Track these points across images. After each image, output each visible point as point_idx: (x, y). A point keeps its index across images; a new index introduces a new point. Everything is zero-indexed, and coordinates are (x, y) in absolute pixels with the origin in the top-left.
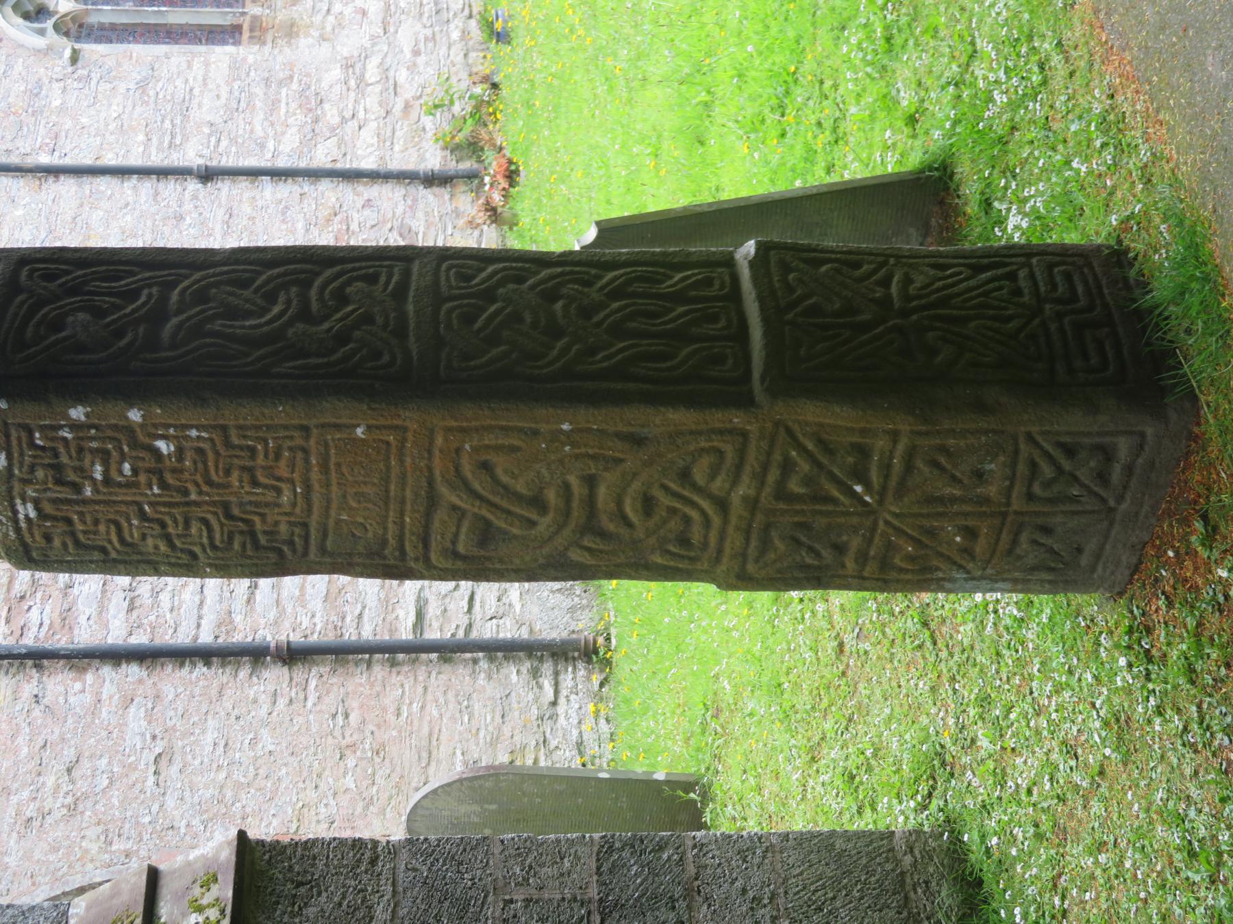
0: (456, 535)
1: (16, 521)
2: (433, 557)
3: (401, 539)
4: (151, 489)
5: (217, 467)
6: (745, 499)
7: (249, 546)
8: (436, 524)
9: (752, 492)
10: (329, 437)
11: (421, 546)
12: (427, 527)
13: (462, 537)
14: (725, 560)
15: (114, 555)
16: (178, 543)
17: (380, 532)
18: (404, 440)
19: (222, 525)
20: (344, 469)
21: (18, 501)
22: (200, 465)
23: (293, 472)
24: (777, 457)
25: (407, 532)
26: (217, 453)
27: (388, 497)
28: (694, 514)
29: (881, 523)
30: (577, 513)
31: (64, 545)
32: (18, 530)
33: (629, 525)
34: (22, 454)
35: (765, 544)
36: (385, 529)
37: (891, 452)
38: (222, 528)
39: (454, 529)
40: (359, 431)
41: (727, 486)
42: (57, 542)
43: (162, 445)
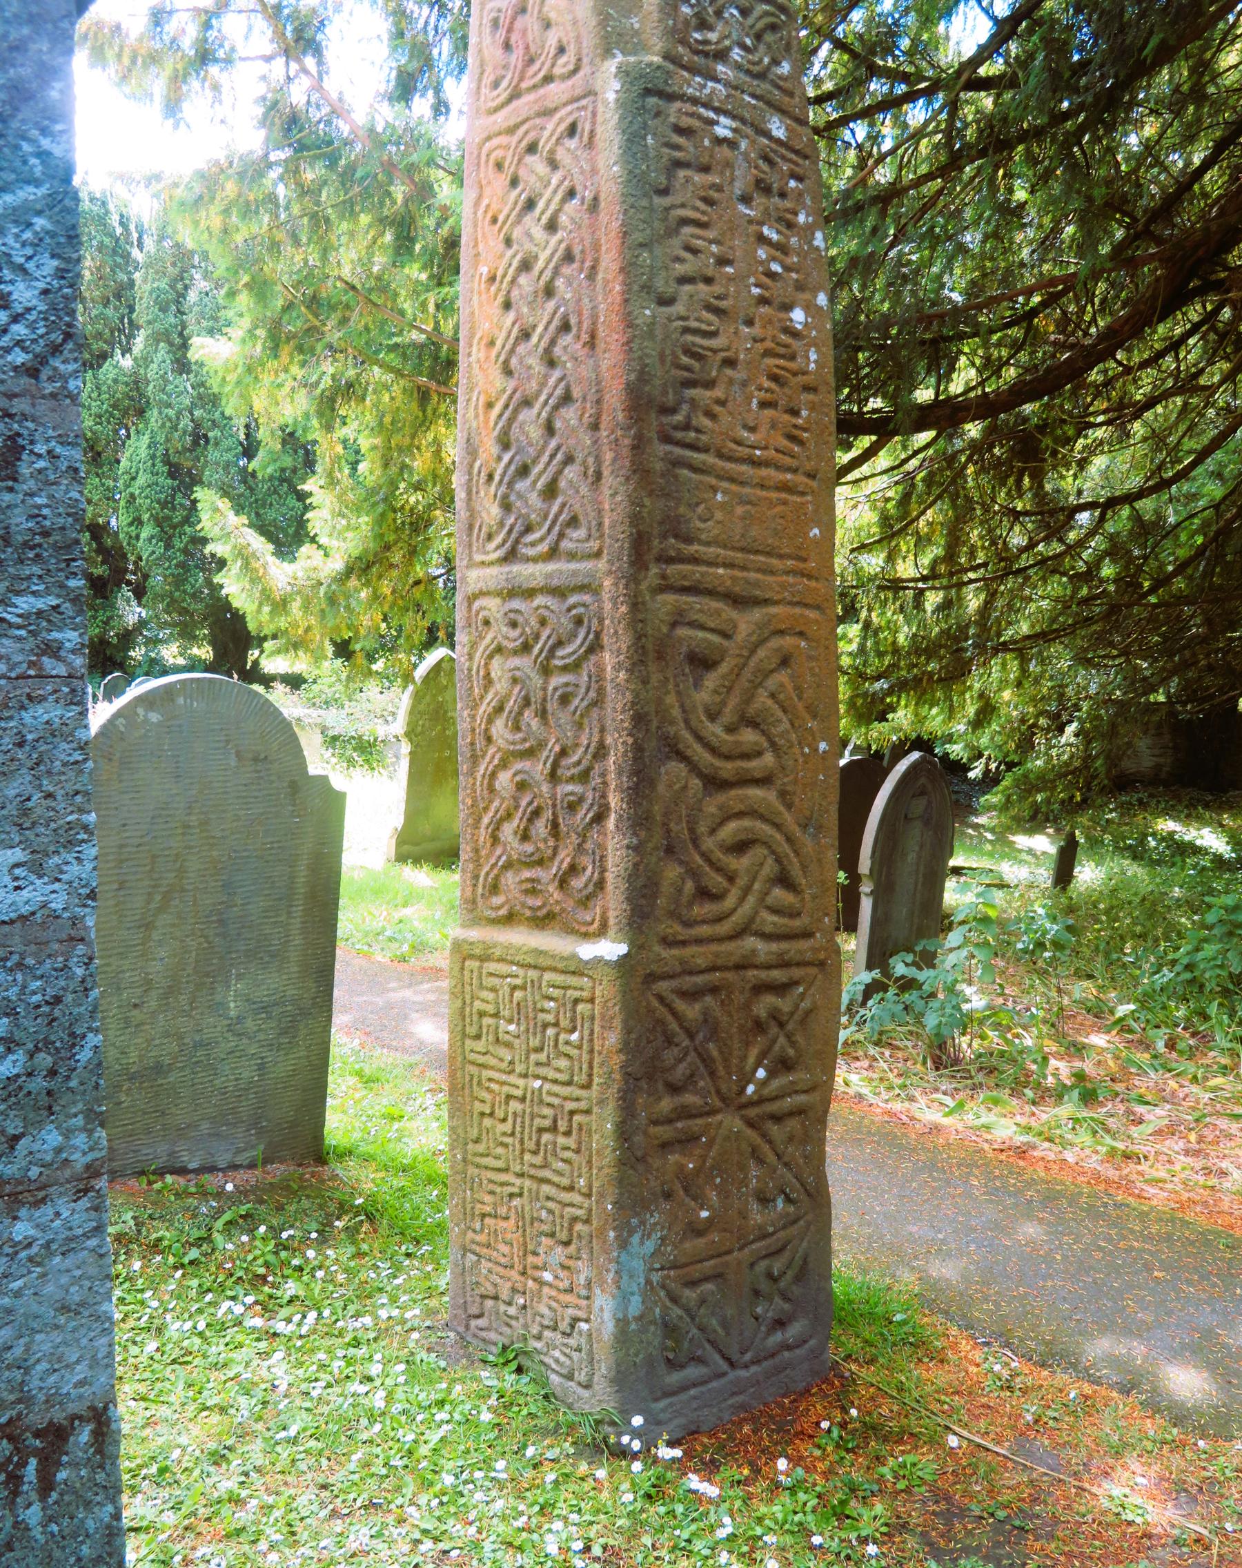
0: (702, 627)
1: (706, 105)
2: (670, 598)
3: (695, 560)
4: (757, 285)
5: (783, 368)
6: (754, 952)
7: (686, 374)
8: (715, 604)
9: (762, 958)
10: (809, 498)
11: (686, 583)
12: (711, 593)
13: (701, 634)
14: (675, 952)
15: (657, 200)
16: (688, 288)
17: (703, 537)
18: (810, 577)
19: (715, 351)
20: (779, 509)
21: (734, 125)
22: (782, 351)
23: (777, 450)
24: (797, 973)
25: (703, 569)
26: (795, 374)
27: (749, 552)
28: (730, 902)
29: (719, 1117)
30: (728, 769)
31: (677, 147)
32: (695, 101)
33: (713, 831)
34: (783, 157)
35: (691, 995)
36: (708, 544)
37: (796, 1092)
38: (711, 350)
39: (712, 625)
40: (816, 531)
41: (768, 929)
42: (680, 140)
43: (798, 315)
